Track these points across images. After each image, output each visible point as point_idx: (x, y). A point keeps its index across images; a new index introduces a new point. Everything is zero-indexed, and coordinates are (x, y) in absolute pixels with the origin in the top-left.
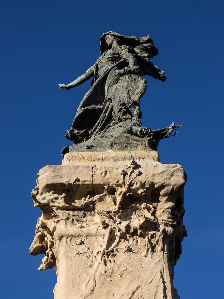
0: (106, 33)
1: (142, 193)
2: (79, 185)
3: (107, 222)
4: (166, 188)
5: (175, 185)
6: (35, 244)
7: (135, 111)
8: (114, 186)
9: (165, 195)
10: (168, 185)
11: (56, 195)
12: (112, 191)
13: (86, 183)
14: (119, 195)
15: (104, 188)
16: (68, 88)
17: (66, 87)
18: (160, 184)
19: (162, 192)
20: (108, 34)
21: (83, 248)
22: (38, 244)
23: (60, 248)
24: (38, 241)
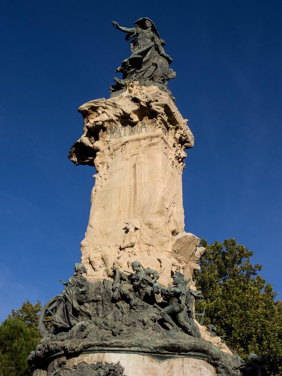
1: (183, 139)
2: (173, 115)
3: (175, 145)
4: (188, 144)
5: (191, 145)
6: (84, 107)
7: (166, 83)
8: (180, 127)
9: (185, 146)
10: (190, 143)
11: (164, 112)
12: (177, 129)
13: (175, 117)
14: (179, 133)
15: (176, 125)
16: (117, 27)
18: (189, 140)
19: (186, 144)
20: (150, 21)
21: (165, 151)
22: (87, 109)
23: (160, 144)
24: (89, 107)
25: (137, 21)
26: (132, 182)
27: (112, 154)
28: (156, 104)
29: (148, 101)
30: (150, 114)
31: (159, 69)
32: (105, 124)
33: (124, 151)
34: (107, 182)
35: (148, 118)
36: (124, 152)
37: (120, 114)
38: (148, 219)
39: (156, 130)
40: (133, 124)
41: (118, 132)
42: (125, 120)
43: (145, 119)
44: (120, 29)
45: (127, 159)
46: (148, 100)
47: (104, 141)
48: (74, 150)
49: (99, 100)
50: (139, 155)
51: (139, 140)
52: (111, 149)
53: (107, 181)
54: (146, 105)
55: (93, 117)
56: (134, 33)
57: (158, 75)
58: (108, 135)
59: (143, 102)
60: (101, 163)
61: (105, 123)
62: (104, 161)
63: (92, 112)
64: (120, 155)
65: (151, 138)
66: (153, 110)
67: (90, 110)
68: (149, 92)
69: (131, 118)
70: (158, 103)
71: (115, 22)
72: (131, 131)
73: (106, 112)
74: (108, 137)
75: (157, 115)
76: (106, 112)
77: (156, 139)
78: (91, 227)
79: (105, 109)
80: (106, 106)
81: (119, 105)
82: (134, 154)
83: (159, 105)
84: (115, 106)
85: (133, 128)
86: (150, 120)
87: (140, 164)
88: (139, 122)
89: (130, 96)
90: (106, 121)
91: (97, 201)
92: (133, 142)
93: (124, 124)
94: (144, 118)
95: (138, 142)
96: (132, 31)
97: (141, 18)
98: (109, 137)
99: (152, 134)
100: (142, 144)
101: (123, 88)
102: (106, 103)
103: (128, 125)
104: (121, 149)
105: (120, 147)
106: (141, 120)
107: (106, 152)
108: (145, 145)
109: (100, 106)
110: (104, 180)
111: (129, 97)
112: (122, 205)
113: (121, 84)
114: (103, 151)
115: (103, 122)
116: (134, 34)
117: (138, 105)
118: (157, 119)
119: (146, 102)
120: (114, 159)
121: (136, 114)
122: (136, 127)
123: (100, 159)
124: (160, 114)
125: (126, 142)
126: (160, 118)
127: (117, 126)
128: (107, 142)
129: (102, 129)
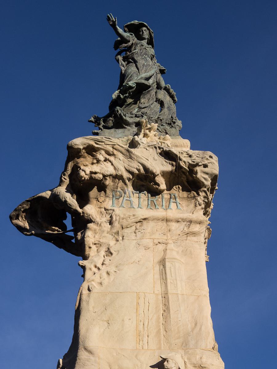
0: (148, 27)
6: (79, 142)
16: (114, 26)
17: (116, 25)
22: (82, 147)
25: (129, 23)
26: (159, 289)
27: (118, 233)
28: (204, 171)
29: (193, 163)
30: (186, 184)
31: (165, 110)
32: (106, 179)
33: (140, 233)
34: (112, 280)
35: (181, 188)
36: (139, 234)
37: (139, 170)
38: (198, 357)
39: (197, 211)
40: (155, 192)
41: (128, 199)
42: (144, 182)
43: (175, 189)
44: (116, 30)
45: (147, 248)
46: (194, 162)
47: (100, 208)
48: (27, 207)
49: (104, 139)
50: (169, 246)
51: (167, 220)
52: (116, 224)
53: (112, 277)
54: (188, 167)
55: (87, 163)
56: (129, 41)
57: (165, 120)
58: (107, 199)
59: (185, 162)
60: (95, 244)
61: (107, 178)
62: (101, 240)
63: (86, 154)
64: (134, 238)
65: (189, 223)
66: (198, 179)
67: (84, 150)
68: (177, 146)
69: (157, 181)
70: (206, 170)
71: (111, 16)
72: (151, 203)
73: (110, 162)
74: (108, 203)
75: (201, 188)
76: (110, 162)
77: (198, 225)
78: (90, 352)
79: (109, 154)
80: (112, 152)
81: (137, 156)
82: (159, 243)
83: (207, 174)
84: (130, 155)
85: (154, 199)
86: (184, 192)
87: (172, 262)
88: (166, 192)
89: (159, 147)
90: (110, 175)
91: (93, 307)
92: (155, 221)
93: (138, 188)
94: (174, 187)
95: (165, 223)
96: (128, 39)
97: (136, 21)
98: (111, 202)
99: (187, 215)
100: (173, 228)
101: (126, 127)
102: (115, 147)
103: (146, 192)
104: (134, 228)
105: (133, 225)
106: (169, 188)
107: (105, 227)
108: (179, 232)
109: (103, 148)
110: (105, 275)
111: (156, 148)
112: (142, 323)
113: (126, 120)
114: (100, 225)
115: (104, 176)
116: (129, 44)
117: (172, 165)
118: (198, 195)
119: (190, 164)
120: (120, 241)
121: (164, 178)
122: (160, 198)
123: (94, 237)
124: (205, 187)
125: (145, 219)
126: (204, 194)
127: (126, 188)
128: (106, 209)
129: (96, 187)
